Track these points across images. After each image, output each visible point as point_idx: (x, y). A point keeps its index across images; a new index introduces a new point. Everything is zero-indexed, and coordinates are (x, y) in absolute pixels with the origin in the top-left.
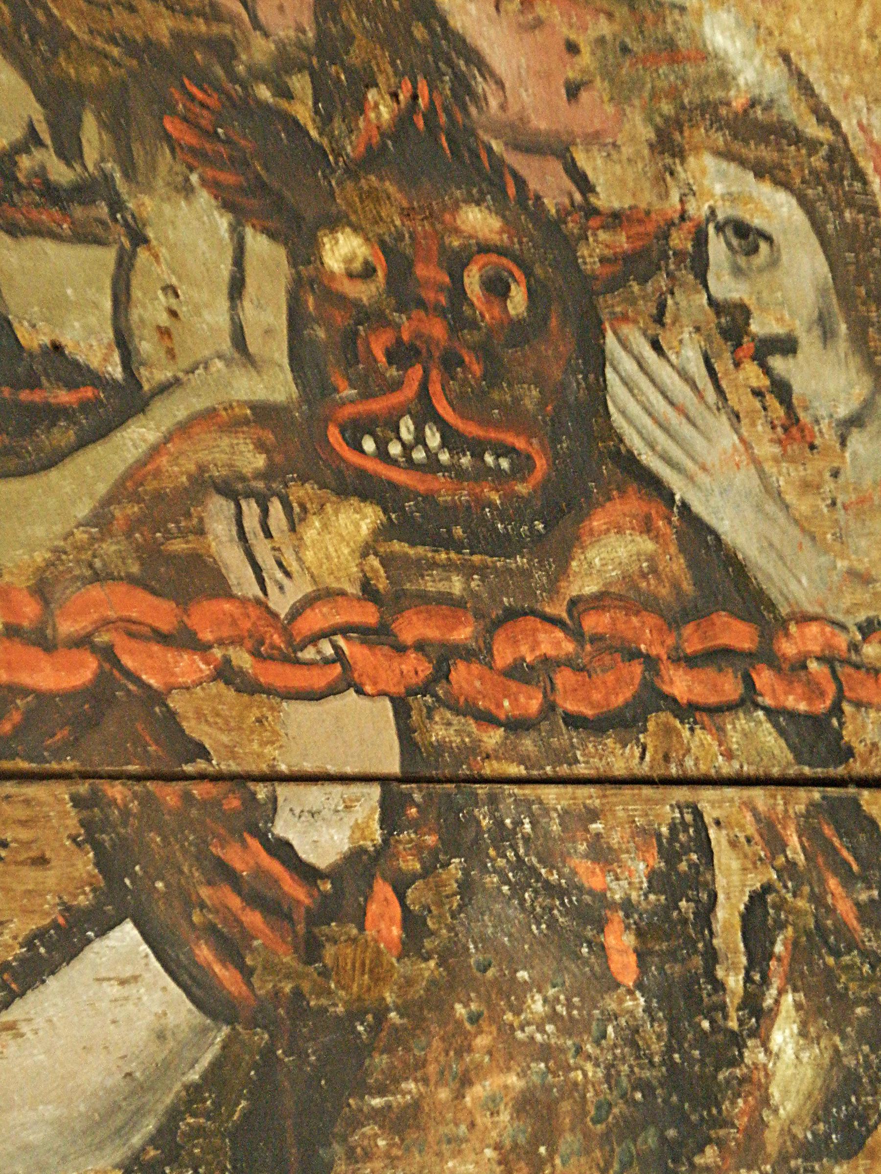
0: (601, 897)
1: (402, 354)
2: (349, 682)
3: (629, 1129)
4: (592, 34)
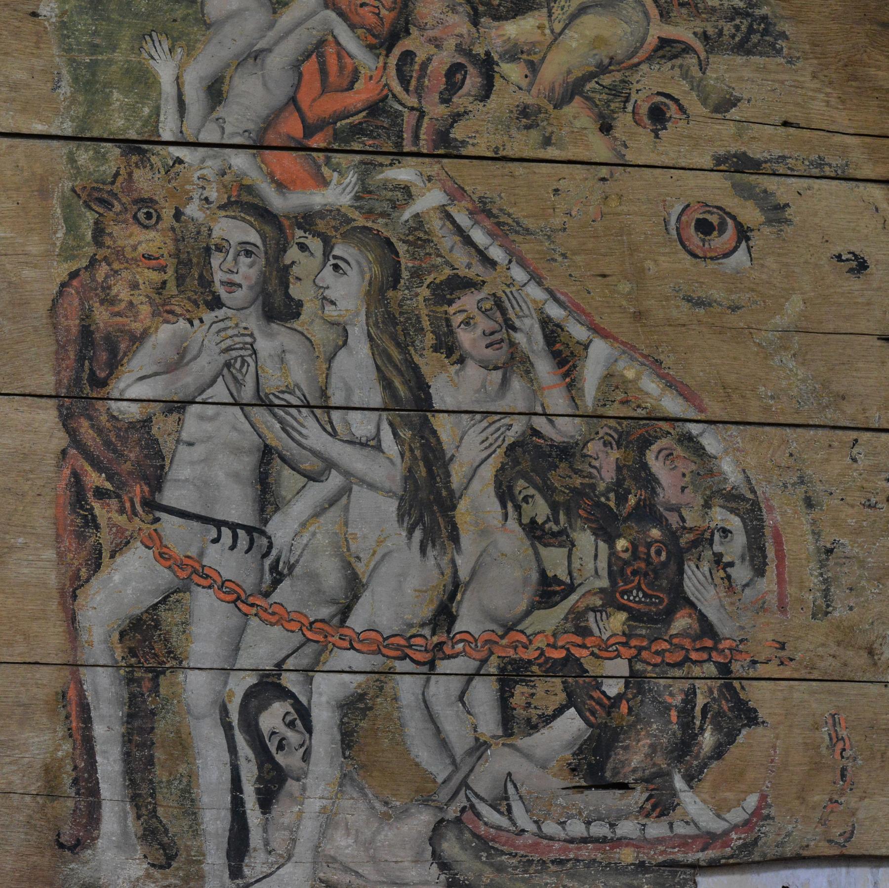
0: (670, 704)
1: (635, 573)
2: (619, 656)
3: (672, 752)
4: (690, 470)
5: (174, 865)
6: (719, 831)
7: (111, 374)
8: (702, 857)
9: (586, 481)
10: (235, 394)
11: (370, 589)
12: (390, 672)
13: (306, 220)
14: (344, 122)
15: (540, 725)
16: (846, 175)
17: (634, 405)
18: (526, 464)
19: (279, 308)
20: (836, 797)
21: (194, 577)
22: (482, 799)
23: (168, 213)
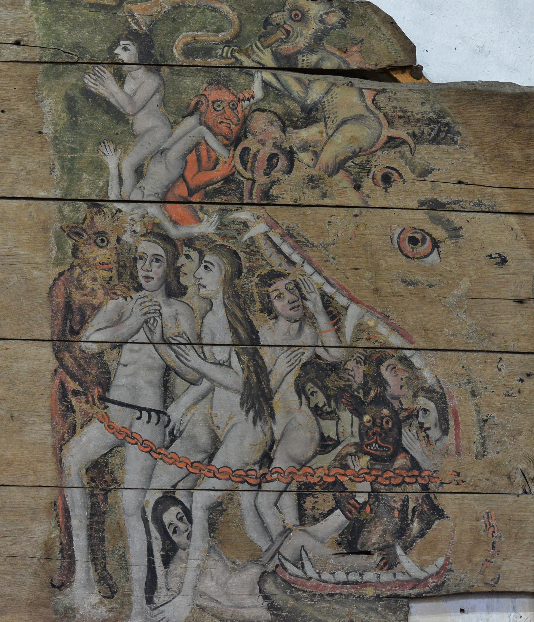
1: (374, 434)
2: (365, 480)
3: (395, 534)
5: (116, 596)
6: (422, 578)
7: (82, 327)
8: (413, 592)
9: (347, 383)
10: (150, 338)
11: (224, 444)
12: (236, 490)
13: (190, 242)
14: (210, 187)
15: (321, 519)
16: (494, 210)
17: (373, 341)
18: (312, 375)
19: (174, 290)
20: (489, 559)
21: (127, 438)
22: (287, 560)
23: (113, 239)
